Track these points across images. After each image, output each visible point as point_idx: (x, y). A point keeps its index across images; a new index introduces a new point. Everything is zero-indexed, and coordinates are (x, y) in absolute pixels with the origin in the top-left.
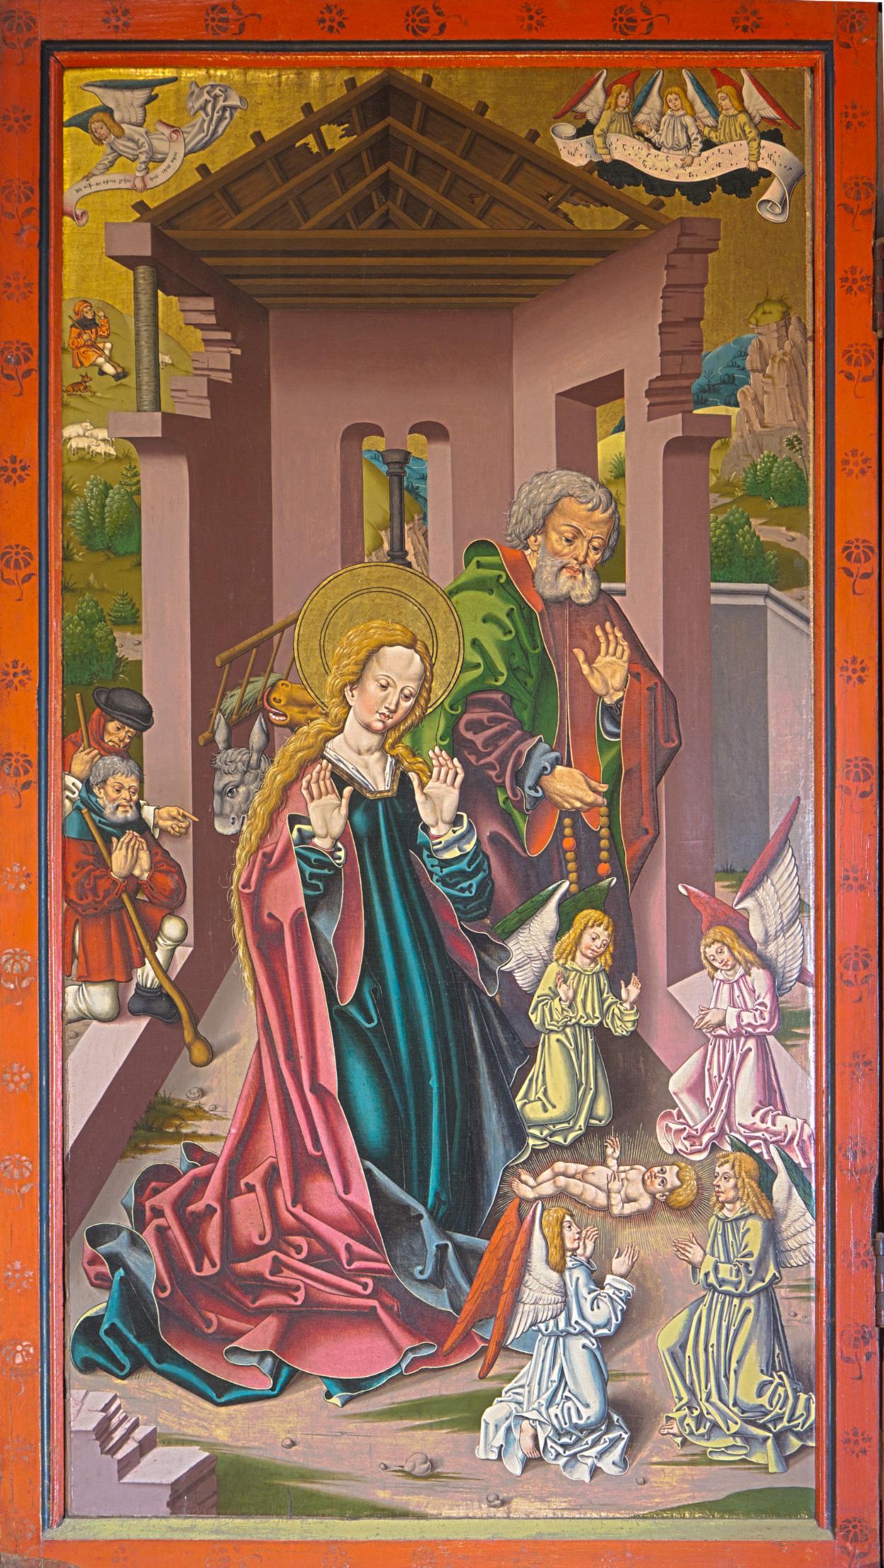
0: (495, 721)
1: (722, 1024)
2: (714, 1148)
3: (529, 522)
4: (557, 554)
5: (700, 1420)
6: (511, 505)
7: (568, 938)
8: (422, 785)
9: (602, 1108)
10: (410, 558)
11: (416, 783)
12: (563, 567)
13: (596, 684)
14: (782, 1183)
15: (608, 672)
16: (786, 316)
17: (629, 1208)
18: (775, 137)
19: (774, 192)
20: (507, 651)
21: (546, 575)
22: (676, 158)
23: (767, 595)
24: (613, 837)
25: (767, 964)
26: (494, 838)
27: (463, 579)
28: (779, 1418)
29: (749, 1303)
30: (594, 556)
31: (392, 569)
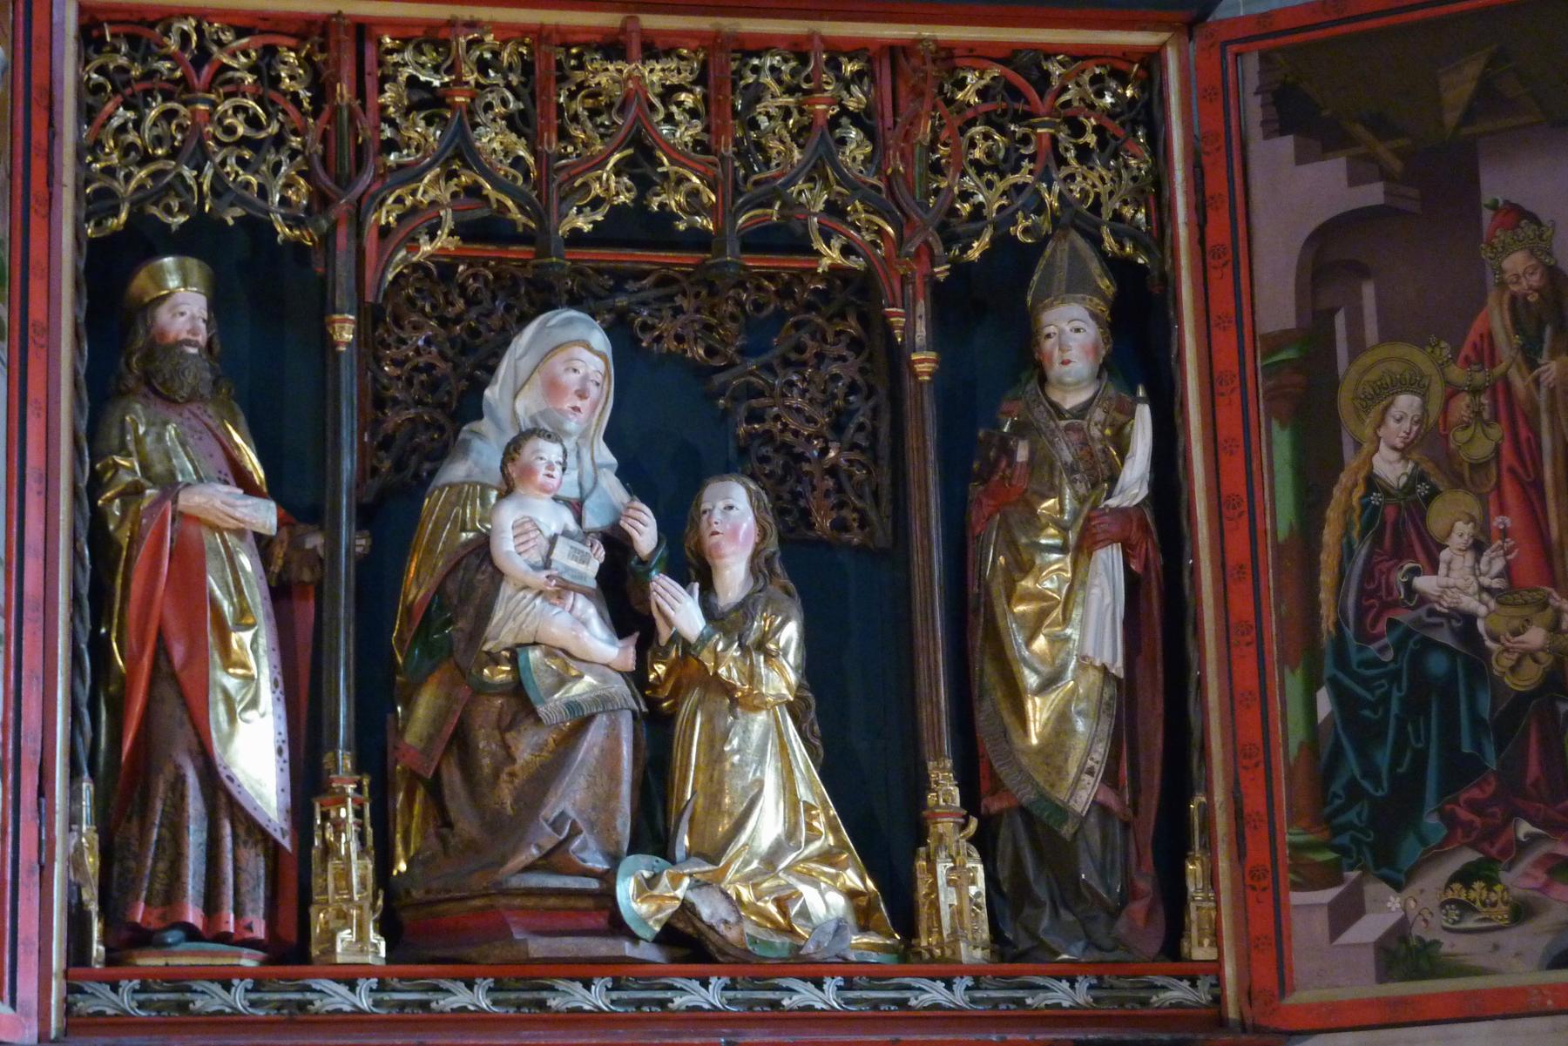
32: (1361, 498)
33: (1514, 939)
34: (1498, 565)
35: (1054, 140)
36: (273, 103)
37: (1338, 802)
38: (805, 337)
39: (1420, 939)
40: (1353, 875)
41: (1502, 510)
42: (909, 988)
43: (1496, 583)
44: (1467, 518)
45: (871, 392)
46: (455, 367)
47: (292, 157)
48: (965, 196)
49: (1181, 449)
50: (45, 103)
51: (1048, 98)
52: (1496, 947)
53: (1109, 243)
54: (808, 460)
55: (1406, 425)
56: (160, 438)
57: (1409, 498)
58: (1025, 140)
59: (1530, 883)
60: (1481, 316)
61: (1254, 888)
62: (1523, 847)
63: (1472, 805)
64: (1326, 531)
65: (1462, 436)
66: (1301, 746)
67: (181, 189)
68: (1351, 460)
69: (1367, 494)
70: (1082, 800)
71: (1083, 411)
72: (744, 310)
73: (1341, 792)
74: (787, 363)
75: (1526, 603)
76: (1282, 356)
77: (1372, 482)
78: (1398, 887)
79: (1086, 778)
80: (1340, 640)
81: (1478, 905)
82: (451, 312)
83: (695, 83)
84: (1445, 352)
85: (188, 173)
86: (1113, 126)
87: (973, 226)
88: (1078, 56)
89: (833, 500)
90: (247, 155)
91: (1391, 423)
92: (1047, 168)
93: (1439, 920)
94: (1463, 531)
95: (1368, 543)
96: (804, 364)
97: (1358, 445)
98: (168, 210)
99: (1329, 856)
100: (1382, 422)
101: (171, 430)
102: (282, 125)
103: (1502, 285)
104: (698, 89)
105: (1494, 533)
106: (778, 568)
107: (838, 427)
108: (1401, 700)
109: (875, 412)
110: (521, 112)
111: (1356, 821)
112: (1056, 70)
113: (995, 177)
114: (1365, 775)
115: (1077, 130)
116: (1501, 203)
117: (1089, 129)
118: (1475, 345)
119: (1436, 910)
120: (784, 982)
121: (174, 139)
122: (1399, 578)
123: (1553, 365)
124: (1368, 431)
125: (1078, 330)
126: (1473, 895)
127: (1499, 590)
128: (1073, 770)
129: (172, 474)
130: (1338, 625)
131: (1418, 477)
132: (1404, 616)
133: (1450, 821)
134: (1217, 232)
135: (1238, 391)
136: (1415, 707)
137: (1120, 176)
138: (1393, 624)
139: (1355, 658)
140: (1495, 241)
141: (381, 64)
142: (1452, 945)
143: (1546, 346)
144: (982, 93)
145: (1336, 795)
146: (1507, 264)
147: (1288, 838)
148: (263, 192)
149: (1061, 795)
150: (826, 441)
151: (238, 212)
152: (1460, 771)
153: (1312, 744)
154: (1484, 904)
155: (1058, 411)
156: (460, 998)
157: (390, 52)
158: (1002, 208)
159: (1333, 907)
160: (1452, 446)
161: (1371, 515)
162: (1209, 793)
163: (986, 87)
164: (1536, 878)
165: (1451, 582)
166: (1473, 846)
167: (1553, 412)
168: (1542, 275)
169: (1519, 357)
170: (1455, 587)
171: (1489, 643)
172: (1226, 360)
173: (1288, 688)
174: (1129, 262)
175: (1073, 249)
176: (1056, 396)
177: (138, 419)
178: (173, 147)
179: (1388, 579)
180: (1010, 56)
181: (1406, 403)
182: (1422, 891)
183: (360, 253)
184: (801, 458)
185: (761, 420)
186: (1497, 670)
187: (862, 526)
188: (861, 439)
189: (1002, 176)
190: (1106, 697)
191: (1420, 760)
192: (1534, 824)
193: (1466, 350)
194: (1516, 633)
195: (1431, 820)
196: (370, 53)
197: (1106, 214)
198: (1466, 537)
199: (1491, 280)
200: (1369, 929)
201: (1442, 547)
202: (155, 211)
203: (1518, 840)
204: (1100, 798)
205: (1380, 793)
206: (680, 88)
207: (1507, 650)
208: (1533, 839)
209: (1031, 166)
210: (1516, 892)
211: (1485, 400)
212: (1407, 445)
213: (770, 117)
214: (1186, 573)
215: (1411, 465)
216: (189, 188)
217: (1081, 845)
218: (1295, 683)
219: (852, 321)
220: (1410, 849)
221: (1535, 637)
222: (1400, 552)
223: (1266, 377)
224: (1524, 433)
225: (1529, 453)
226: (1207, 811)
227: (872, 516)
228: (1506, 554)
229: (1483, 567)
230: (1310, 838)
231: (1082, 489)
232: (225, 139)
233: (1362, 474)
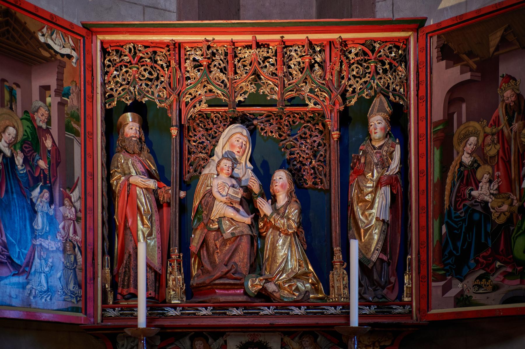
0: (29, 147)
1: (67, 217)
2: (66, 240)
3: (35, 110)
4: (39, 117)
5: (64, 292)
6: (32, 105)
7: (42, 194)
8: (16, 157)
9: (48, 229)
10: (14, 110)
11: (15, 156)
12: (41, 120)
13: (46, 145)
14: (77, 249)
15: (48, 144)
16: (76, 85)
17: (52, 249)
18: (74, 50)
19: (74, 60)
20: (31, 134)
21: (38, 121)
22: (59, 47)
23: (74, 137)
24: (50, 176)
25: (75, 207)
26: (29, 171)
27: (23, 117)
28: (76, 294)
29: (72, 271)
30: (46, 120)
31: (10, 111)
32: (458, 169)
33: (493, 295)
34: (496, 187)
35: (376, 67)
36: (156, 68)
37: (446, 257)
38: (307, 131)
39: (466, 295)
40: (450, 277)
41: (498, 170)
42: (324, 309)
43: (495, 192)
44: (488, 173)
45: (325, 145)
46: (210, 143)
47: (161, 83)
48: (350, 86)
49: (409, 157)
50: (91, 69)
51: (375, 54)
52: (488, 298)
53: (391, 97)
54: (306, 165)
55: (472, 146)
56: (127, 164)
57: (472, 168)
58: (368, 68)
59: (499, 280)
60: (497, 111)
61: (422, 281)
62: (497, 269)
63: (484, 257)
64: (448, 179)
65: (488, 148)
66: (437, 241)
67: (130, 93)
68: (456, 158)
69: (460, 167)
70: (374, 258)
71: (381, 147)
72: (290, 123)
73: (447, 254)
74: (301, 137)
75: (503, 198)
76: (439, 128)
77: (461, 164)
78: (461, 281)
79: (376, 251)
80: (449, 211)
81: (483, 286)
82: (208, 127)
83: (273, 56)
84: (485, 123)
85: (132, 89)
86: (394, 63)
87: (353, 95)
88: (384, 41)
89: (313, 176)
90: (149, 83)
91: (468, 146)
92: (373, 76)
93: (472, 290)
95: (459, 182)
96: (307, 138)
97: (458, 153)
98: (126, 99)
99: (443, 272)
100: (465, 146)
101: (130, 162)
102: (158, 74)
103: (503, 101)
104: (274, 58)
105: (495, 177)
106: (294, 195)
107: (315, 156)
108: (465, 227)
109: (326, 150)
110: (225, 67)
111: (451, 263)
112: (377, 45)
113: (358, 79)
114: (454, 249)
115: (383, 64)
116: (505, 75)
117: (387, 63)
118: (494, 120)
119: (472, 287)
120: (290, 308)
121: (128, 79)
122: (467, 192)
123: (517, 124)
124: (461, 149)
125: (379, 123)
126: (482, 283)
127: (496, 194)
128: (373, 250)
129: (130, 173)
130: (449, 206)
131: (475, 161)
132: (468, 203)
133: (477, 261)
135: (425, 139)
137: (396, 78)
138: (465, 205)
139: (453, 215)
140: (502, 87)
141: (186, 55)
142: (476, 297)
143: (515, 119)
144: (356, 55)
145: (446, 255)
146: (505, 94)
147: (432, 267)
148: (153, 94)
149: (369, 256)
150: (311, 159)
151: (146, 99)
153: (440, 241)
154: (485, 286)
155: (374, 148)
156: (204, 312)
157: (188, 51)
158: (360, 89)
159: (443, 286)
160: (485, 152)
161: (460, 173)
162: (412, 255)
163: (358, 53)
164: (500, 278)
165: (482, 192)
166: (483, 269)
167: (515, 139)
168: (515, 97)
169: (507, 123)
170: (483, 194)
171: (491, 210)
172: (422, 131)
173: (435, 226)
174: (398, 104)
175: (381, 100)
176: (373, 143)
177: (121, 158)
178: (128, 81)
179: (464, 192)
182: (468, 282)
183: (180, 110)
184: (304, 165)
185: (293, 154)
186: (493, 218)
187: (321, 184)
188: (322, 159)
189: (361, 79)
190: (383, 229)
191: (470, 244)
192: (501, 263)
193: (491, 122)
194: (500, 207)
196: (182, 51)
197: (391, 89)
198: (487, 179)
199: (500, 99)
200: (453, 292)
201: (480, 182)
202: (123, 100)
203: (496, 267)
204: (380, 257)
205: (458, 254)
206: (269, 58)
207: (497, 212)
208: (500, 267)
209: (369, 75)
210: (494, 282)
211: (495, 137)
212: (472, 152)
213: (295, 65)
214: (409, 193)
215: (473, 158)
216: (132, 93)
217: (375, 270)
218: (436, 223)
219: (320, 124)
220: (465, 270)
221: (505, 208)
222: (468, 184)
223: (434, 135)
224: (506, 146)
225: (506, 151)
226: (411, 260)
227: (324, 179)
228: (498, 183)
229: (491, 188)
230: (438, 267)
231: (379, 170)
232: (142, 78)
233: (458, 162)
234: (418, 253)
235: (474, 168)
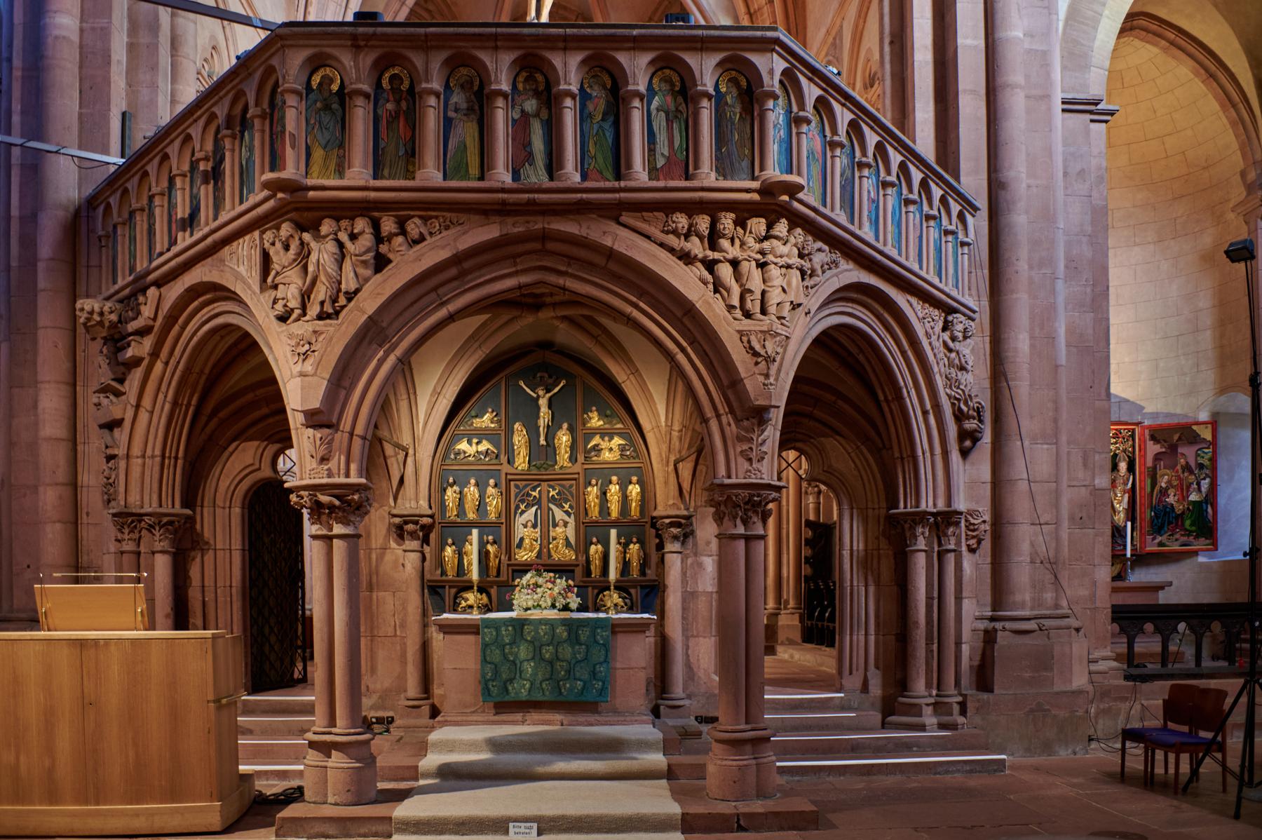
33: (1176, 543)
88: (1125, 429)
94: (1173, 494)
134: (1142, 453)
136: (1165, 515)
142: (1167, 543)
152: (1170, 523)
161: (1161, 491)
180: (1116, 430)
181: (1166, 477)
195: (1166, 529)
220: (1163, 532)
221: (1181, 507)
225: (1182, 485)
234: (1141, 523)
235: (1166, 489)
